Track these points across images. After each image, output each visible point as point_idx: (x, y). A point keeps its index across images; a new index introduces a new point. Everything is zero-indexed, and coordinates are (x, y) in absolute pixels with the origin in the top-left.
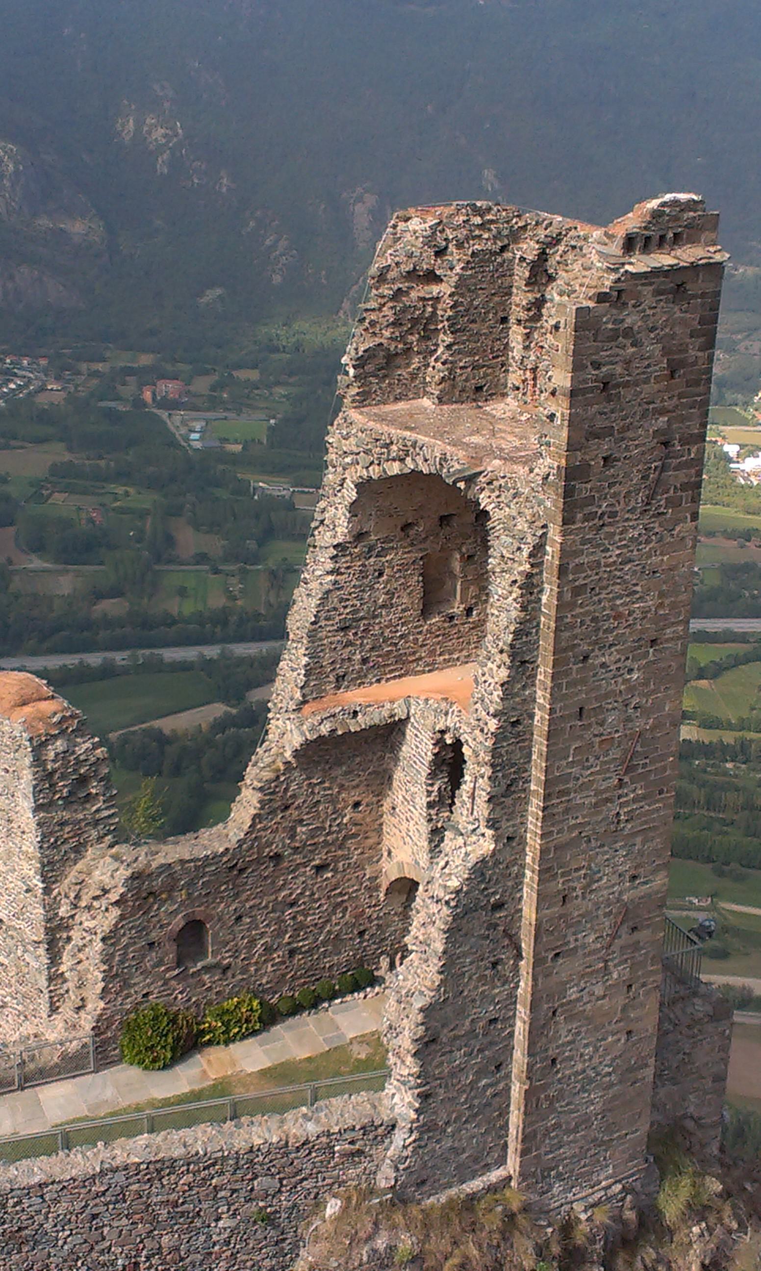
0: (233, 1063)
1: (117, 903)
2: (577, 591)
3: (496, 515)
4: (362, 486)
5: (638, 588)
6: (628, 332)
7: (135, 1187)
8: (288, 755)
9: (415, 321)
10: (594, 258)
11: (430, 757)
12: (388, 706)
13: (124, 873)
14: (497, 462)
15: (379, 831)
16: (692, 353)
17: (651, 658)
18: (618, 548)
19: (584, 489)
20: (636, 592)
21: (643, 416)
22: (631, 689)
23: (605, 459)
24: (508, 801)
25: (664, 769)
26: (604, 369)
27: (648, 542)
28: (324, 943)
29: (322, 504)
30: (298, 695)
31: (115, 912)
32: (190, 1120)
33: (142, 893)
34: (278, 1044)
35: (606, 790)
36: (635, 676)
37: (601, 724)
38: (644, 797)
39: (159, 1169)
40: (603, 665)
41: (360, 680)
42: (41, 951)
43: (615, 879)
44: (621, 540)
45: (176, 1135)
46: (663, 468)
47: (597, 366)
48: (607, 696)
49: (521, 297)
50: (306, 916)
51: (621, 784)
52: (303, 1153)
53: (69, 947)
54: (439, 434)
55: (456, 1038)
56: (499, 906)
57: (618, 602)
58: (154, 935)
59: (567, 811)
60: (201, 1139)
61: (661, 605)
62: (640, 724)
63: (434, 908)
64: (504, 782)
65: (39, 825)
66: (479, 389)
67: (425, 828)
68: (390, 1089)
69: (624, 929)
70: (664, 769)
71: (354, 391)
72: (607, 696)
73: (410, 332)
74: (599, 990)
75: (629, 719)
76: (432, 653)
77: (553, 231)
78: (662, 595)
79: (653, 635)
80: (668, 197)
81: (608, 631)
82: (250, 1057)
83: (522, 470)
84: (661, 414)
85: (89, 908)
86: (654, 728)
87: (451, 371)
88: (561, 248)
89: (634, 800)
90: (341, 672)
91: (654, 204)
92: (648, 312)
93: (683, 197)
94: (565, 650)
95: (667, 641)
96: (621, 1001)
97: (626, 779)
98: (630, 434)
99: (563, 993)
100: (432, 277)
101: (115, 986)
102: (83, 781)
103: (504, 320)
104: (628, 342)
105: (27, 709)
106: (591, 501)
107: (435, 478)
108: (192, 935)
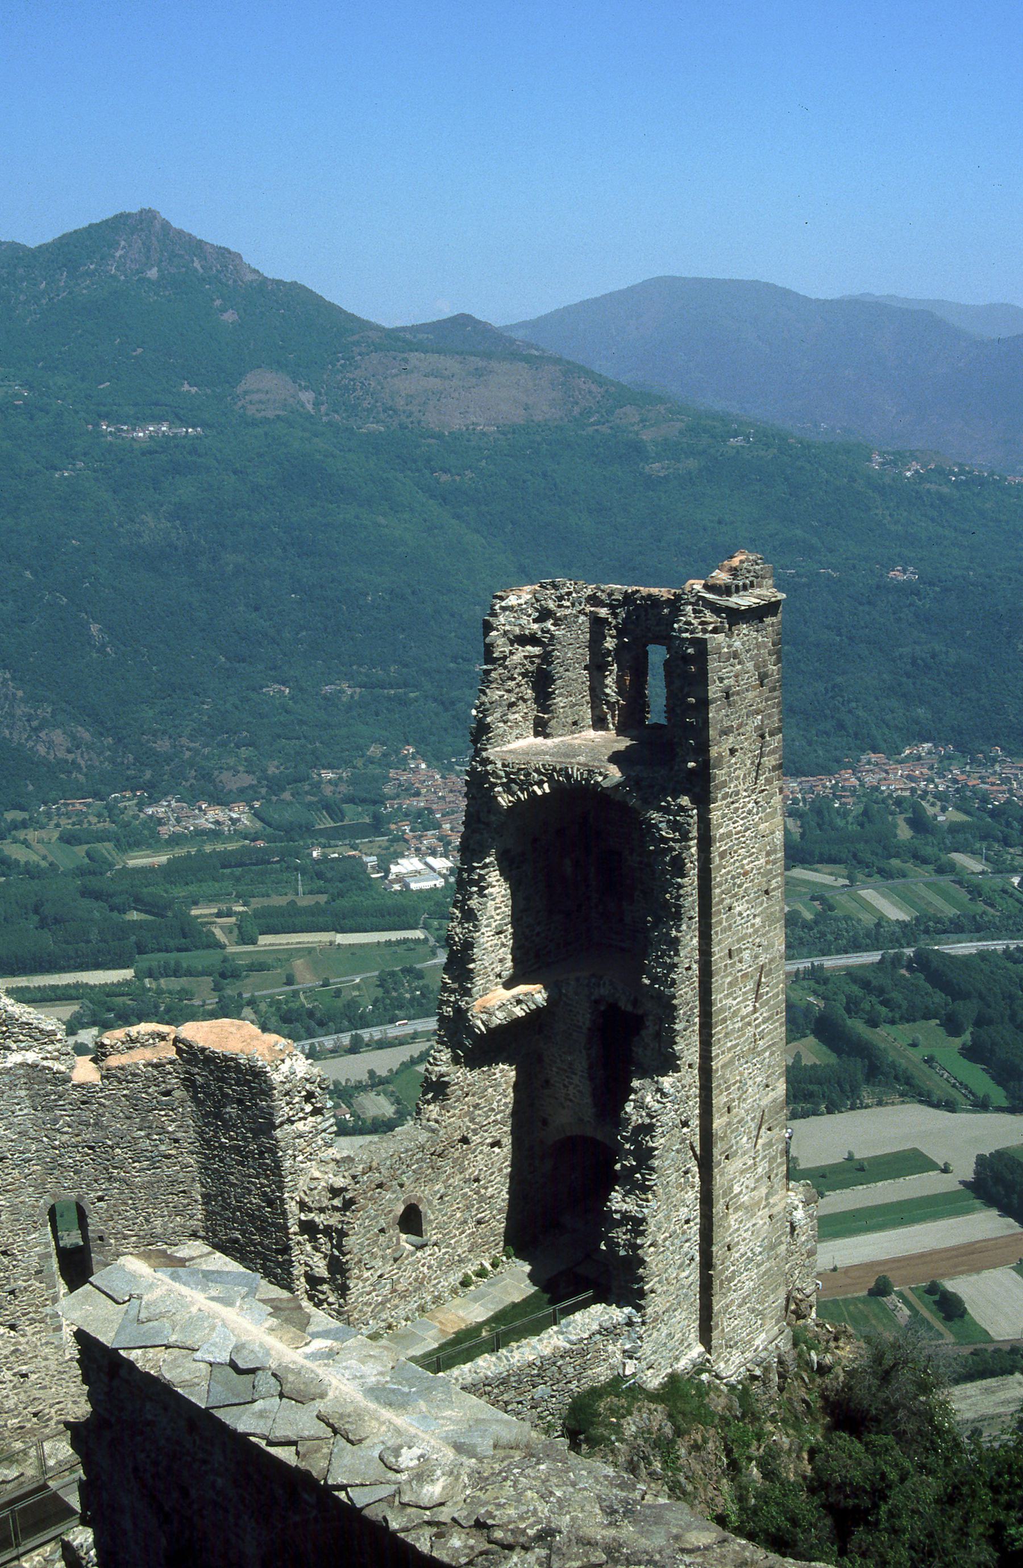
5: (754, 850)
6: (735, 655)
11: (588, 1024)
17: (765, 905)
18: (742, 819)
20: (753, 853)
26: (726, 682)
35: (747, 1016)
44: (743, 813)
46: (761, 755)
48: (742, 938)
50: (486, 1188)
51: (755, 1010)
57: (745, 862)
59: (727, 1035)
62: (762, 960)
66: (575, 723)
72: (742, 938)
75: (756, 957)
78: (768, 854)
81: (740, 886)
84: (758, 714)
89: (764, 1022)
92: (745, 639)
95: (774, 889)
96: (764, 1190)
97: (757, 1005)
99: (731, 1188)
104: (736, 661)
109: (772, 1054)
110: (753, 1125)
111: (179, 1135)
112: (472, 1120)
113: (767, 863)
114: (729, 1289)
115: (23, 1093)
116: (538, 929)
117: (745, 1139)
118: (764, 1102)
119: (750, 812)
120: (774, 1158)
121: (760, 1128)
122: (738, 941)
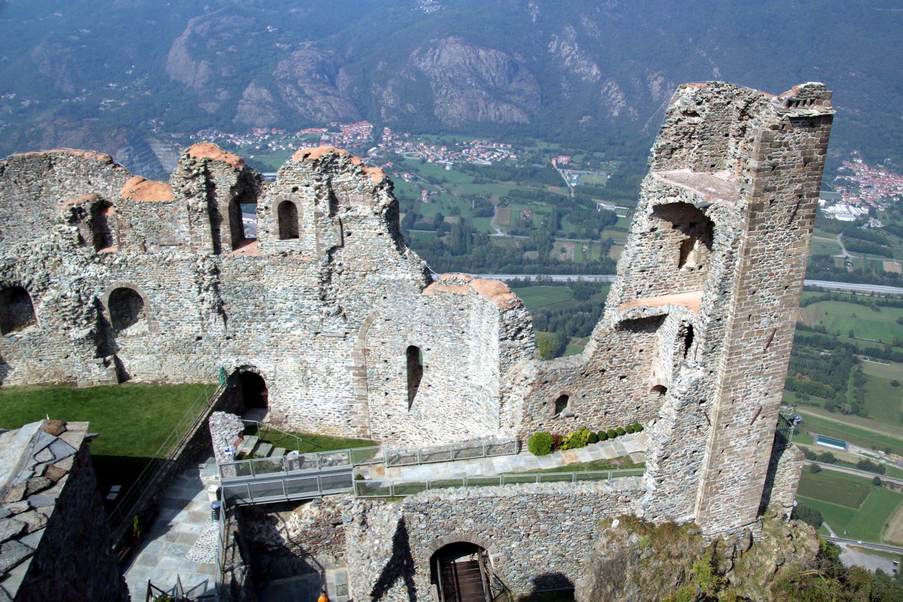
0: (576, 458)
1: (531, 384)
2: (753, 262)
3: (718, 224)
4: (655, 207)
6: (786, 144)
7: (531, 503)
8: (612, 326)
9: (685, 134)
10: (772, 109)
11: (677, 332)
12: (660, 307)
13: (536, 371)
14: (720, 200)
15: (650, 363)
16: (815, 155)
19: (760, 215)
21: (791, 182)
22: (774, 309)
23: (771, 202)
24: (712, 355)
25: (786, 346)
27: (788, 241)
28: (621, 410)
29: (637, 214)
30: (619, 299)
31: (530, 388)
32: (556, 479)
33: (543, 381)
34: (597, 452)
35: (758, 354)
36: (776, 302)
37: (759, 323)
38: (775, 358)
39: (542, 498)
40: (762, 297)
41: (648, 294)
42: (497, 401)
43: (758, 394)
45: (550, 485)
46: (797, 208)
47: (770, 158)
49: (735, 126)
51: (765, 352)
52: (603, 498)
53: (509, 401)
54: (693, 185)
55: (677, 458)
56: (702, 402)
58: (546, 399)
59: (739, 362)
60: (561, 487)
61: (791, 271)
63: (673, 400)
64: (711, 347)
65: (501, 347)
66: (713, 166)
67: (671, 364)
68: (645, 476)
69: (759, 417)
70: (786, 346)
71: (655, 163)
72: (763, 310)
73: (682, 138)
74: (744, 443)
75: (772, 322)
76: (682, 285)
77: (752, 96)
78: (792, 266)
79: (786, 284)
80: (809, 83)
82: (584, 455)
83: (731, 204)
85: (519, 385)
86: (783, 327)
87: (700, 157)
88: (756, 104)
89: (771, 359)
90: (639, 290)
91: (802, 86)
93: (816, 84)
94: (745, 288)
96: (753, 448)
98: (783, 191)
100: (694, 114)
101: (528, 419)
102: (520, 330)
103: (727, 135)
105: (499, 297)
106: (763, 220)
107: (690, 206)
108: (562, 401)
109: (773, 379)
110: (752, 414)
111: (465, 330)
112: (611, 362)
113: (791, 271)
114: (718, 493)
115: (400, 293)
116: (669, 274)
117: (744, 419)
118: (761, 403)
119: (781, 240)
120: (766, 433)
121: (757, 416)
122: (759, 312)
